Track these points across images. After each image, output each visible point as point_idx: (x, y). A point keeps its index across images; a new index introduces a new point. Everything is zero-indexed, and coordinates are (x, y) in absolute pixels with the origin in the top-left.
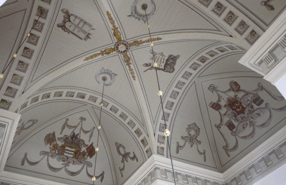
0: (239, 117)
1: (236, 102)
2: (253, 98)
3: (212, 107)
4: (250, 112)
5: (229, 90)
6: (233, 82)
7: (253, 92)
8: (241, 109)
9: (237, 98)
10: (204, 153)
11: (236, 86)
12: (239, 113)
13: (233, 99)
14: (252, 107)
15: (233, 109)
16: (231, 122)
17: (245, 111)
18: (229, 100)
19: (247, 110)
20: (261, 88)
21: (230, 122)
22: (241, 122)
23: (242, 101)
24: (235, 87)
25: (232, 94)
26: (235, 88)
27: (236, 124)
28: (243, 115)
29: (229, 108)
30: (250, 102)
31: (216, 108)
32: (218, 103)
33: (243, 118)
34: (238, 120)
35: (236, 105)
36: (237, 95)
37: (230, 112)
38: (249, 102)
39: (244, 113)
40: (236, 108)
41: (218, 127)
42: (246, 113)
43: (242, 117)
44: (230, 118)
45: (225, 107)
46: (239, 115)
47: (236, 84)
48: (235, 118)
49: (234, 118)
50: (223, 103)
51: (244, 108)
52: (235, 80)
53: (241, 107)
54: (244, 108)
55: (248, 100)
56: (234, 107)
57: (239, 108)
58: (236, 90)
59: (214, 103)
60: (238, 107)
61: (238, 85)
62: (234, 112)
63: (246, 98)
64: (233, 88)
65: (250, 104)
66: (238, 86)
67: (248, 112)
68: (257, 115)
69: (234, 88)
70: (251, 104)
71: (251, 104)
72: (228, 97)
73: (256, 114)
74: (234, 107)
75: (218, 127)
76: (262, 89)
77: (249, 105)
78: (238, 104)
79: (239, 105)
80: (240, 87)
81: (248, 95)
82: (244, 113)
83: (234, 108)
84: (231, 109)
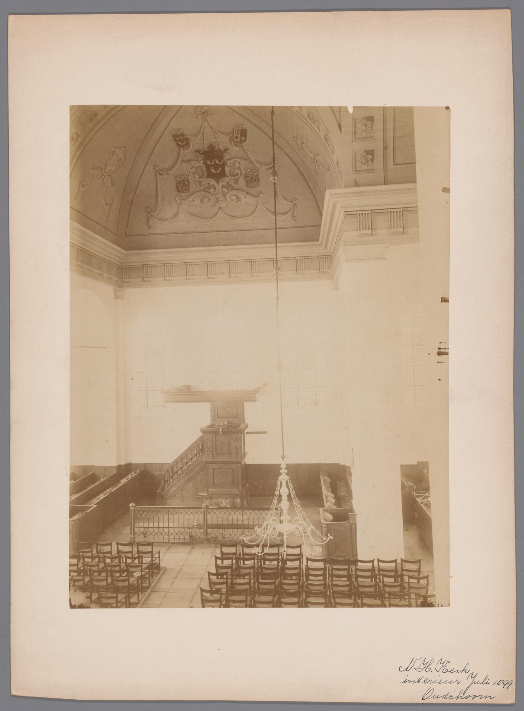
0: (206, 181)
1: (221, 158)
2: (248, 170)
3: (174, 136)
4: (228, 186)
5: (227, 134)
6: (242, 128)
7: (256, 164)
8: (218, 172)
9: (226, 154)
10: (111, 205)
11: (241, 136)
12: (210, 175)
13: (220, 149)
14: (236, 182)
15: (205, 163)
16: (188, 180)
17: (223, 179)
18: (211, 146)
19: (226, 181)
20: (271, 166)
21: (185, 178)
22: (204, 190)
23: (228, 162)
24: (239, 136)
25: (223, 142)
26: (237, 137)
27: (193, 187)
28: (213, 182)
29: (200, 158)
30: (240, 173)
31: (180, 143)
32: (190, 137)
33: (210, 187)
34: (201, 185)
35: (215, 161)
36: (228, 149)
37: (197, 165)
38: (237, 171)
39: (218, 182)
40: (213, 166)
41: (159, 172)
42: (221, 184)
43: (211, 184)
44: (190, 173)
45: (196, 151)
46: (208, 179)
47: (244, 133)
48: (199, 178)
49: (197, 176)
50: (196, 144)
51: (223, 174)
52: (247, 126)
53: (220, 169)
54: (223, 174)
55: (239, 168)
56: (211, 162)
57: (217, 169)
58: (235, 140)
59: (183, 135)
60: (216, 166)
61: (245, 136)
62: (205, 169)
63: (240, 163)
64: (233, 135)
65: (238, 174)
66: (243, 138)
67: (225, 184)
68: (234, 198)
69: (235, 135)
70: (239, 177)
71: (239, 177)
72: (214, 140)
73: (235, 195)
74: (211, 162)
75: (159, 172)
76: (270, 168)
77: (235, 176)
78: (220, 161)
79: (219, 165)
80: (245, 140)
81: (247, 161)
82: (218, 182)
83: (209, 163)
84: (202, 162)
